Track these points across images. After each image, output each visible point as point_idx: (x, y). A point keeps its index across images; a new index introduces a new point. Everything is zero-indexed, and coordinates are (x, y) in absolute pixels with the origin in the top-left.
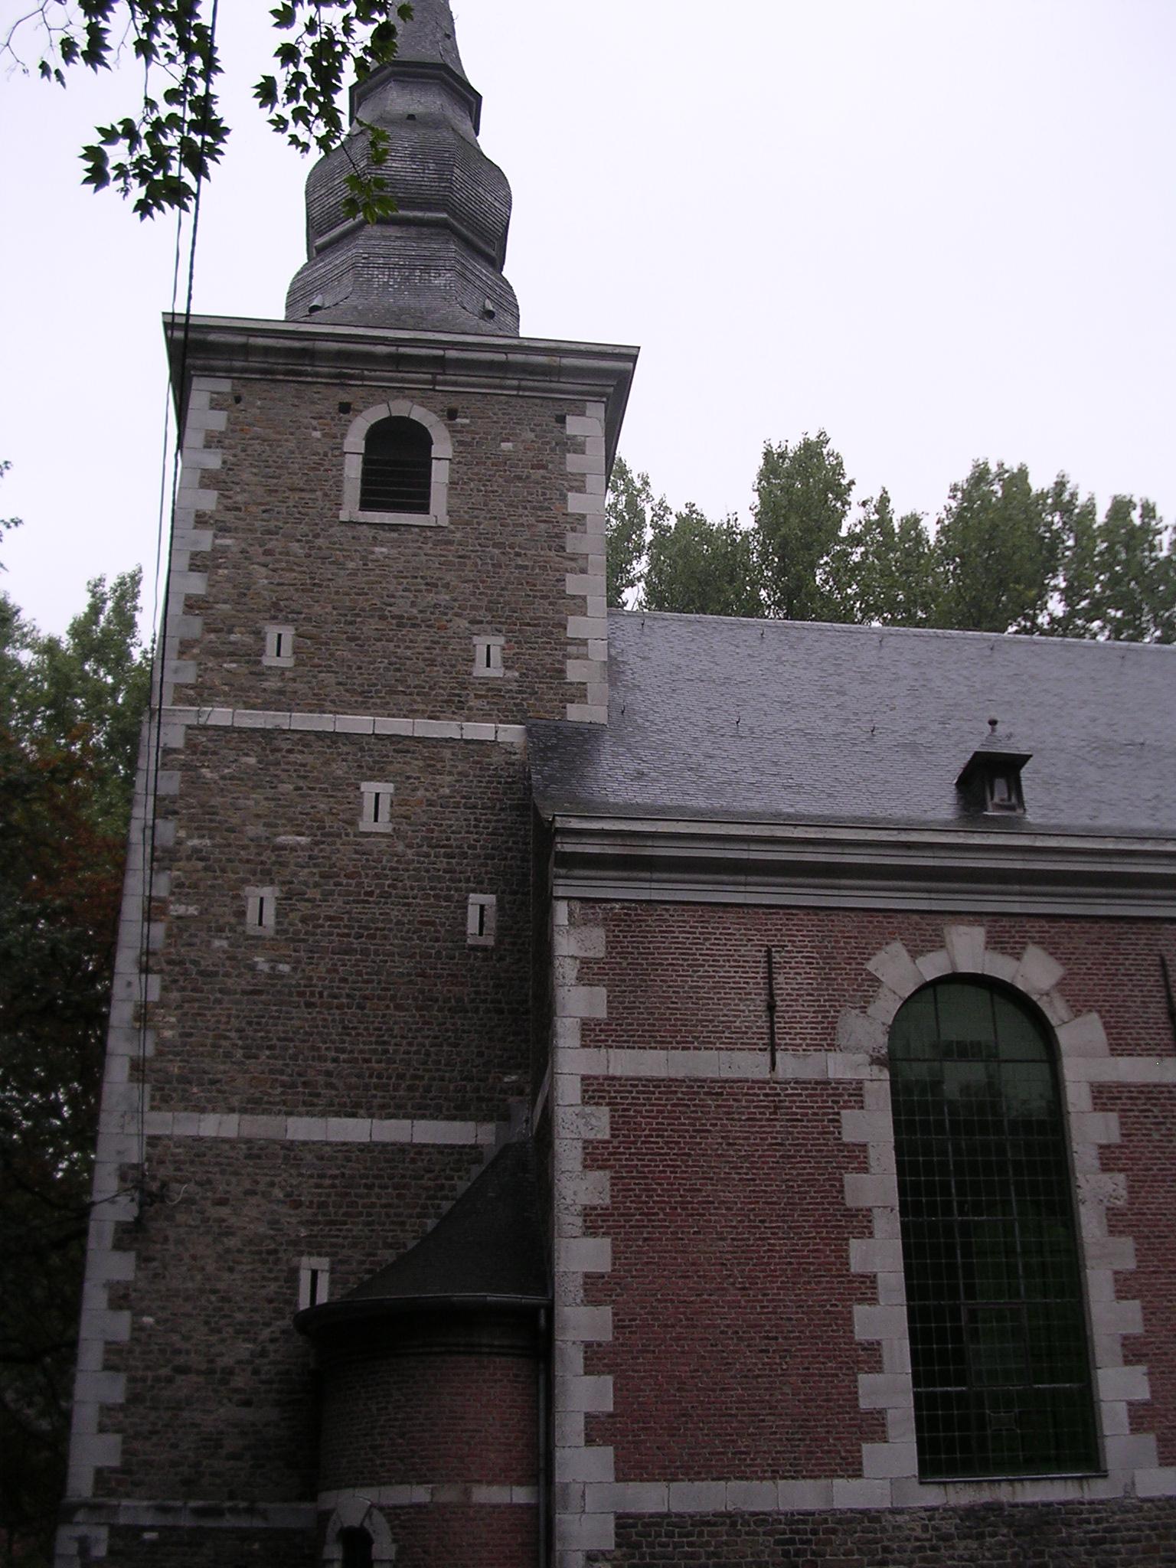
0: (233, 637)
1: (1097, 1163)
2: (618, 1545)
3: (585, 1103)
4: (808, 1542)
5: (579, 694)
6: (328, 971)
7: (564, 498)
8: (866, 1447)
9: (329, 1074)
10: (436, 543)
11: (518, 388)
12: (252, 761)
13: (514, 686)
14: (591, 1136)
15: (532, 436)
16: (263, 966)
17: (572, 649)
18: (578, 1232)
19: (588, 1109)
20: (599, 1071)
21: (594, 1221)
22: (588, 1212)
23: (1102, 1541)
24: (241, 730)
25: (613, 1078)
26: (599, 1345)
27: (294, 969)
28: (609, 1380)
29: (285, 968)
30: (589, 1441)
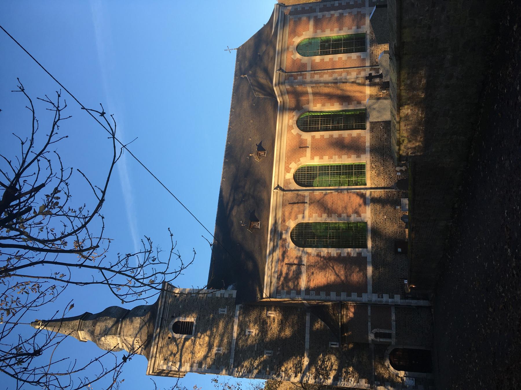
5: (230, 295)
12: (241, 355)
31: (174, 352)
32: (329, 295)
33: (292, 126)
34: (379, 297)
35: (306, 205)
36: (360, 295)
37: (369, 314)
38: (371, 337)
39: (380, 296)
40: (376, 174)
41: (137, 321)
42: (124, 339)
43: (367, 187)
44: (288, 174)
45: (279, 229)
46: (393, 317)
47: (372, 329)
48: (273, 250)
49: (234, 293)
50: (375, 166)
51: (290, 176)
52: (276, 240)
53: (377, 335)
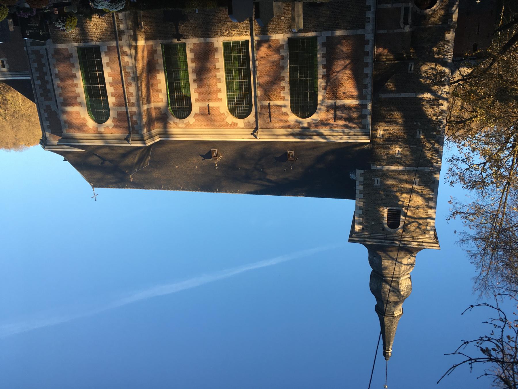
16: (419, 123)
20: (365, 100)
21: (366, 75)
24: (423, 166)
29: (415, 123)
30: (369, 40)
31: (417, 225)
32: (367, 74)
33: (185, 124)
34: (369, 22)
35: (271, 104)
37: (386, 31)
38: (407, 29)
40: (236, 30)
41: (386, 263)
42: (405, 274)
43: (250, 40)
44: (239, 125)
45: (297, 130)
46: (389, 6)
47: (400, 28)
48: (321, 135)
49: (359, 172)
50: (226, 31)
51: (241, 123)
52: (310, 133)
53: (406, 23)
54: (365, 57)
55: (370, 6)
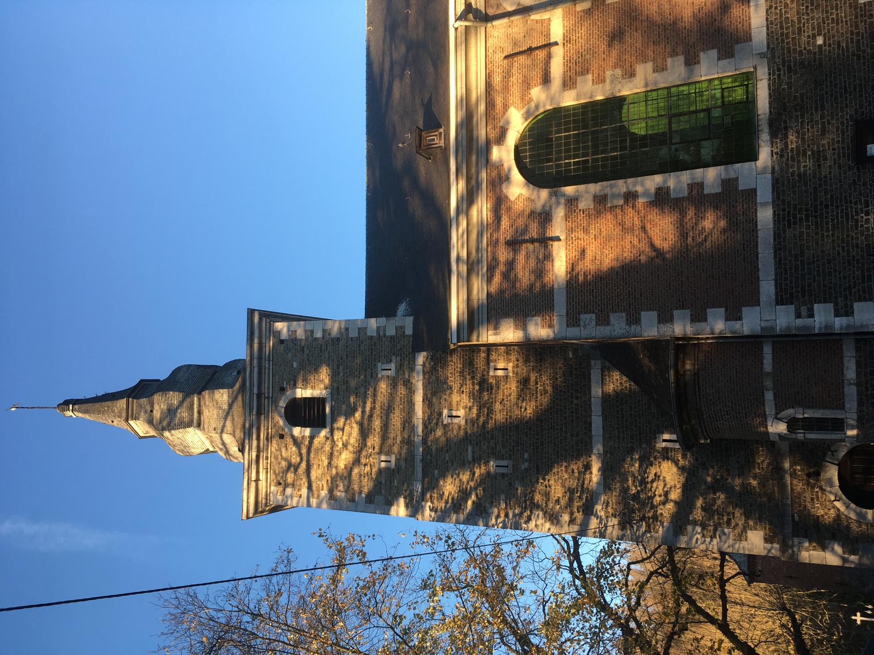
0: (383, 482)
1: (601, 85)
2: (792, 303)
3: (579, 326)
4: (789, 212)
5: (400, 329)
6: (527, 436)
7: (316, 339)
8: (740, 188)
9: (572, 435)
10: (338, 394)
11: (269, 361)
13: (398, 358)
14: (594, 323)
15: (290, 354)
16: (526, 465)
17: (381, 334)
18: (638, 327)
19: (582, 324)
21: (634, 320)
22: (629, 323)
23: (789, 67)
25: (567, 313)
26: (692, 315)
27: (527, 451)
28: (709, 310)
29: (526, 456)
30: (740, 318)
34: (798, 316)
35: (554, 49)
36: (734, 315)
38: (781, 428)
39: (804, 312)
46: (851, 373)
47: (779, 408)
49: (408, 323)
53: (792, 424)
54: (688, 312)
55: (849, 312)
